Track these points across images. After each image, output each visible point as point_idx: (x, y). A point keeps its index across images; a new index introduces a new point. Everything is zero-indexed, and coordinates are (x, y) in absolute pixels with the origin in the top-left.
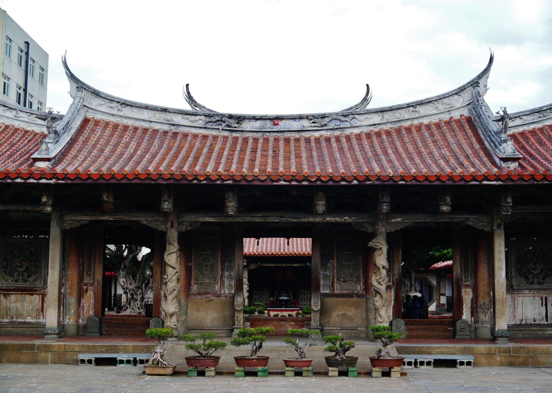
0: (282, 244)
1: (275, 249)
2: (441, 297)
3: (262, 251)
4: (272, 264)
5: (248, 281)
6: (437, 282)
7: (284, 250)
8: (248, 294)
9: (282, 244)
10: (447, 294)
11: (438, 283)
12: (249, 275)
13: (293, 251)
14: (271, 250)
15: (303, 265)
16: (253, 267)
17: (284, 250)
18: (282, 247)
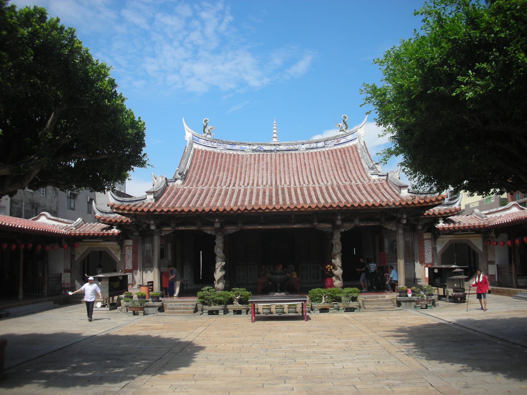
0: (274, 195)
1: (264, 202)
2: (490, 266)
3: (242, 205)
4: (261, 224)
5: (224, 252)
6: (483, 246)
7: (278, 202)
8: (224, 273)
9: (274, 195)
10: (497, 262)
11: (485, 247)
12: (224, 243)
13: (292, 203)
14: (257, 204)
15: (308, 226)
16: (231, 229)
17: (278, 202)
18: (274, 199)
